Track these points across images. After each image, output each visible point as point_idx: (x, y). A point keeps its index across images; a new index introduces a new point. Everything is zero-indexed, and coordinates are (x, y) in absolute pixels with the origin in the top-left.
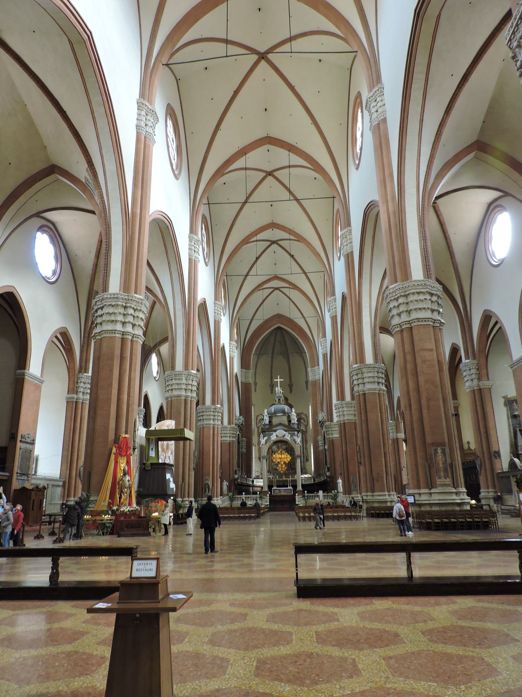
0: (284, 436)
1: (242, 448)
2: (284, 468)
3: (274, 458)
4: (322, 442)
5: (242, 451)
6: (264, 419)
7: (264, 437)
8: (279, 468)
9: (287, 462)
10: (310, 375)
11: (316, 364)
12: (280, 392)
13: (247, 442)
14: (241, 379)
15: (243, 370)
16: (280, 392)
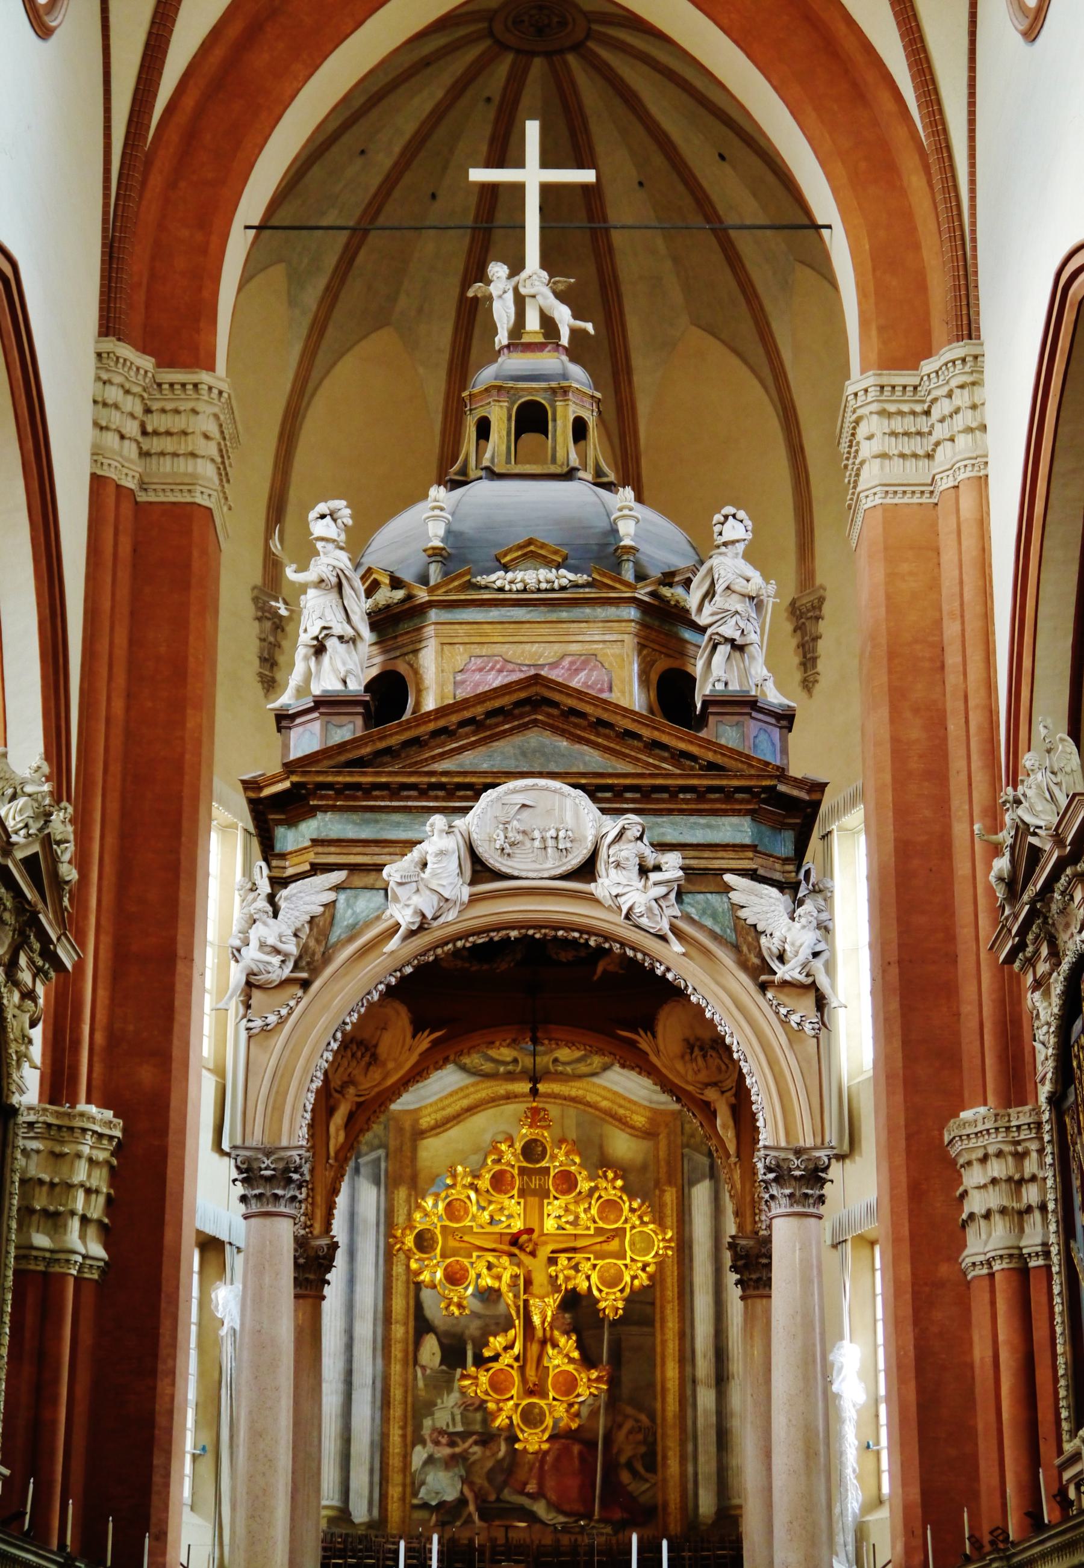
0: (587, 870)
1: (55, 1220)
2: (569, 1385)
3: (424, 1242)
4: (997, 1169)
5: (60, 1254)
6: (309, 628)
7: (279, 883)
8: (498, 1386)
9: (611, 1302)
10: (866, 449)
11: (939, 328)
12: (548, 324)
13: (119, 1150)
14: (97, 453)
15: (125, 351)
16: (548, 324)
